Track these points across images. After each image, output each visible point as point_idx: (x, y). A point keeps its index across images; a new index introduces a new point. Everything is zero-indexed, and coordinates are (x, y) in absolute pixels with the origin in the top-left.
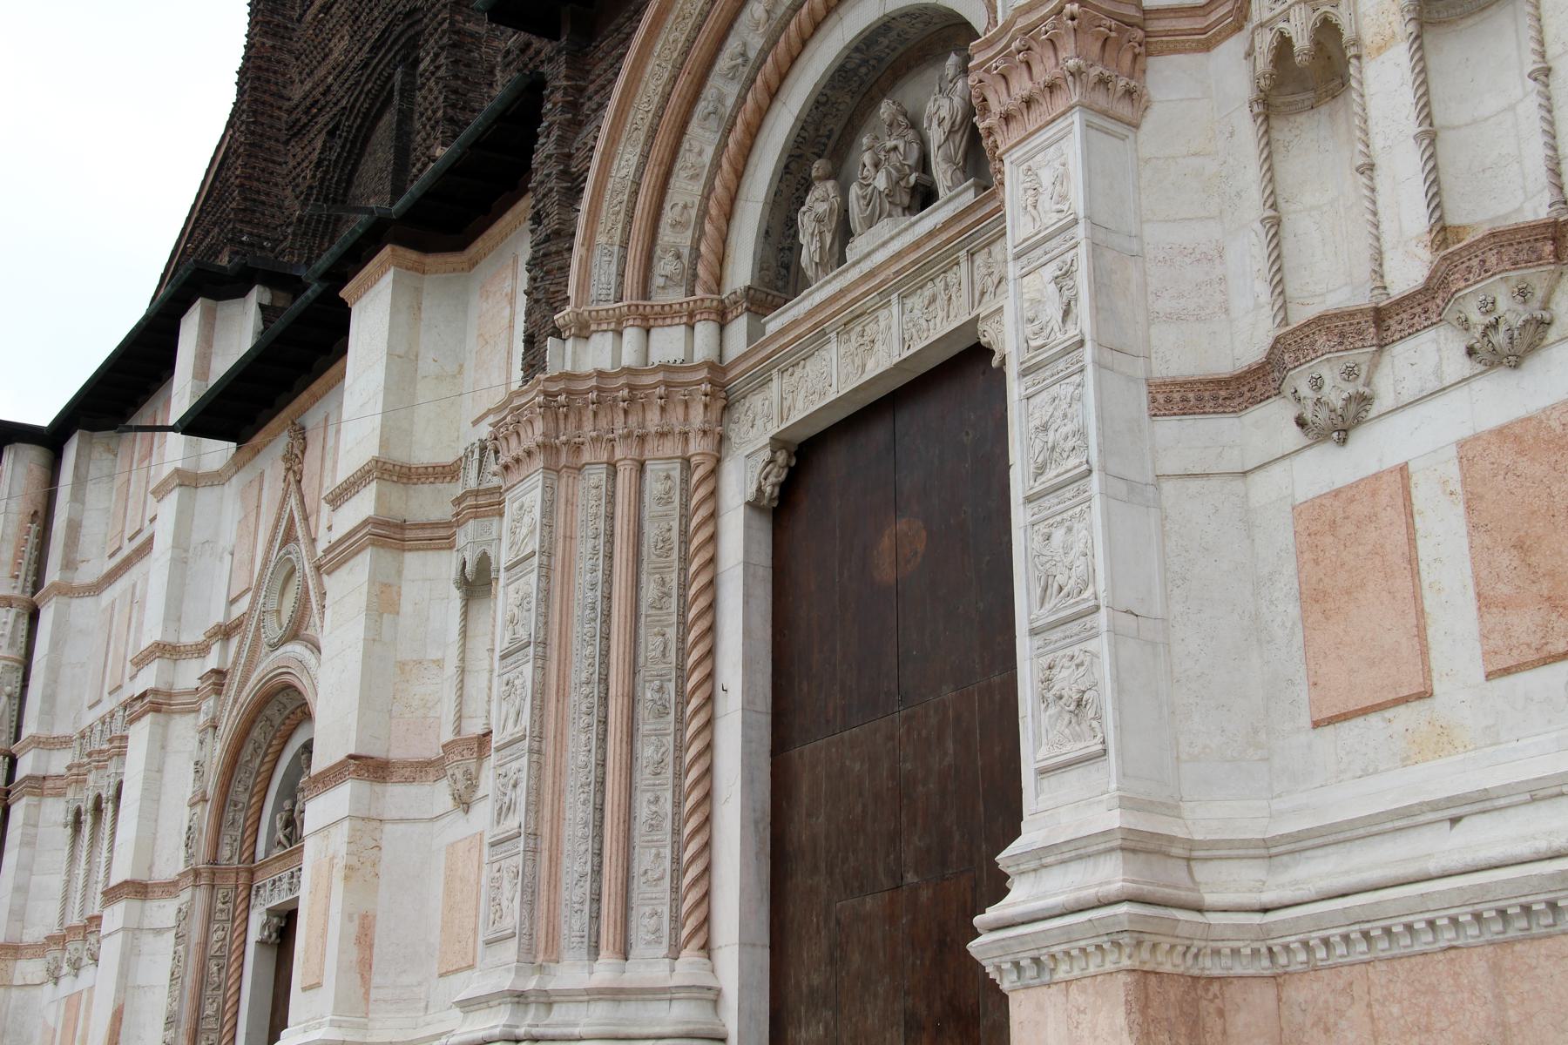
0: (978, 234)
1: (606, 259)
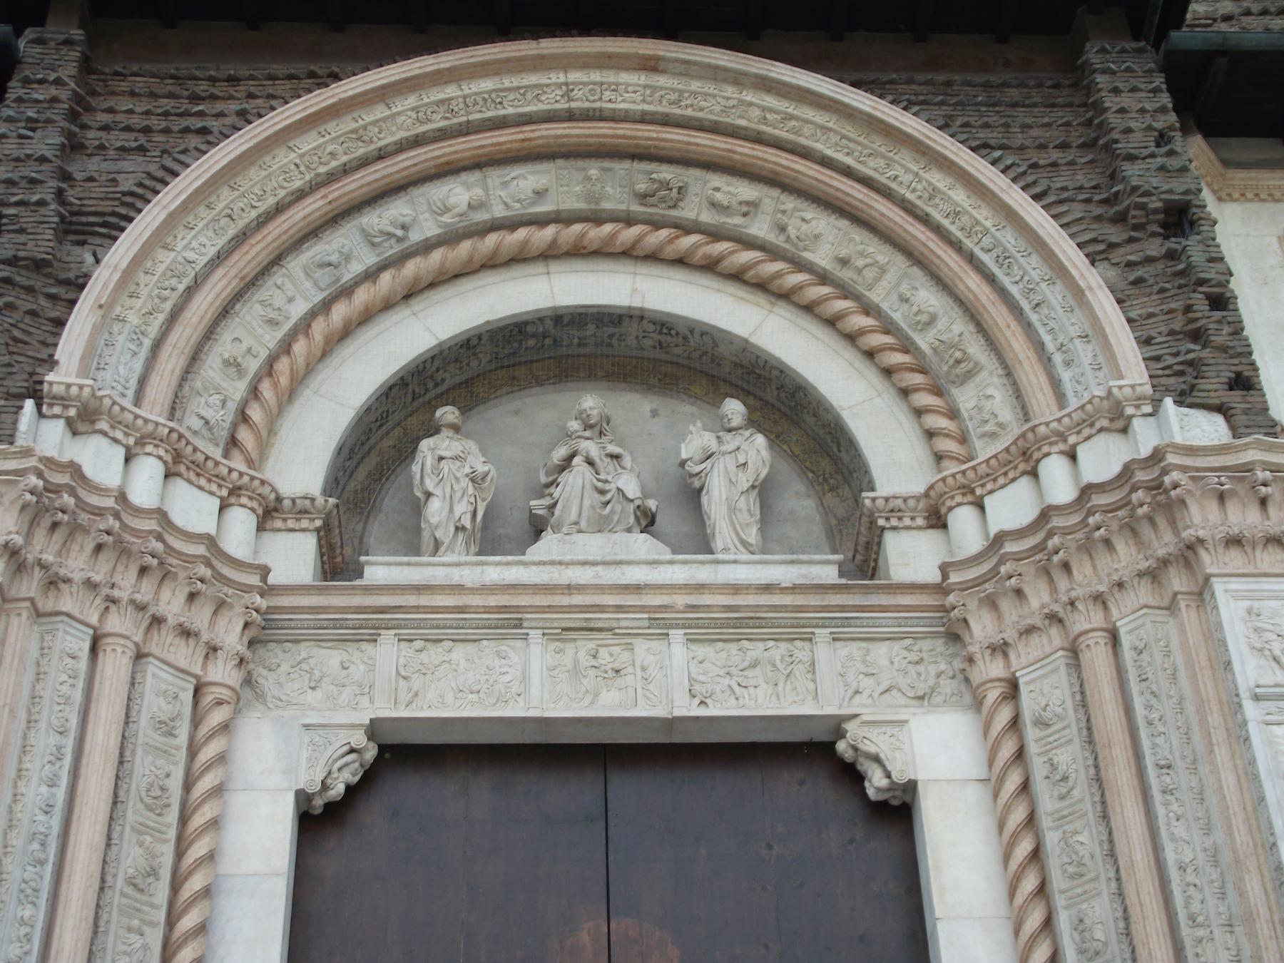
0: (858, 622)
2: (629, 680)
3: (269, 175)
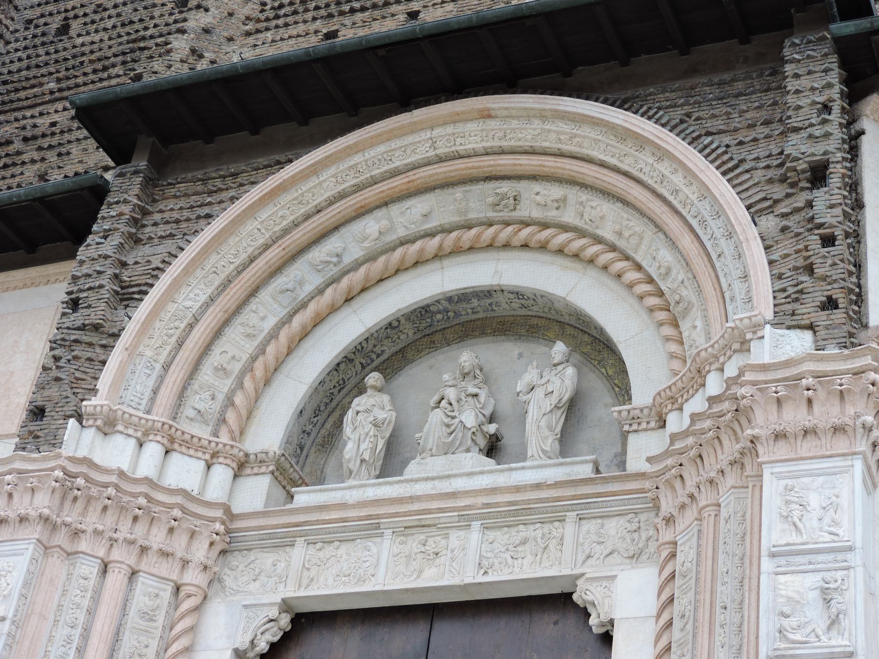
0: (596, 505)
1: (146, 371)
2: (443, 558)
3: (241, 240)
